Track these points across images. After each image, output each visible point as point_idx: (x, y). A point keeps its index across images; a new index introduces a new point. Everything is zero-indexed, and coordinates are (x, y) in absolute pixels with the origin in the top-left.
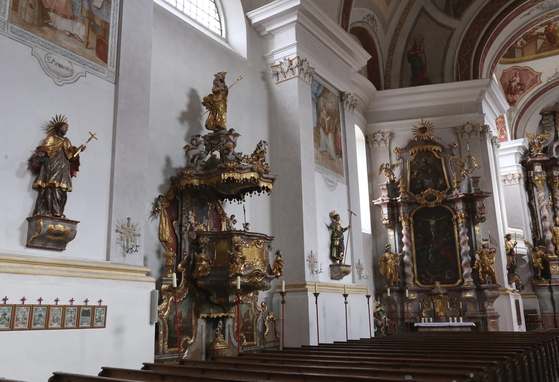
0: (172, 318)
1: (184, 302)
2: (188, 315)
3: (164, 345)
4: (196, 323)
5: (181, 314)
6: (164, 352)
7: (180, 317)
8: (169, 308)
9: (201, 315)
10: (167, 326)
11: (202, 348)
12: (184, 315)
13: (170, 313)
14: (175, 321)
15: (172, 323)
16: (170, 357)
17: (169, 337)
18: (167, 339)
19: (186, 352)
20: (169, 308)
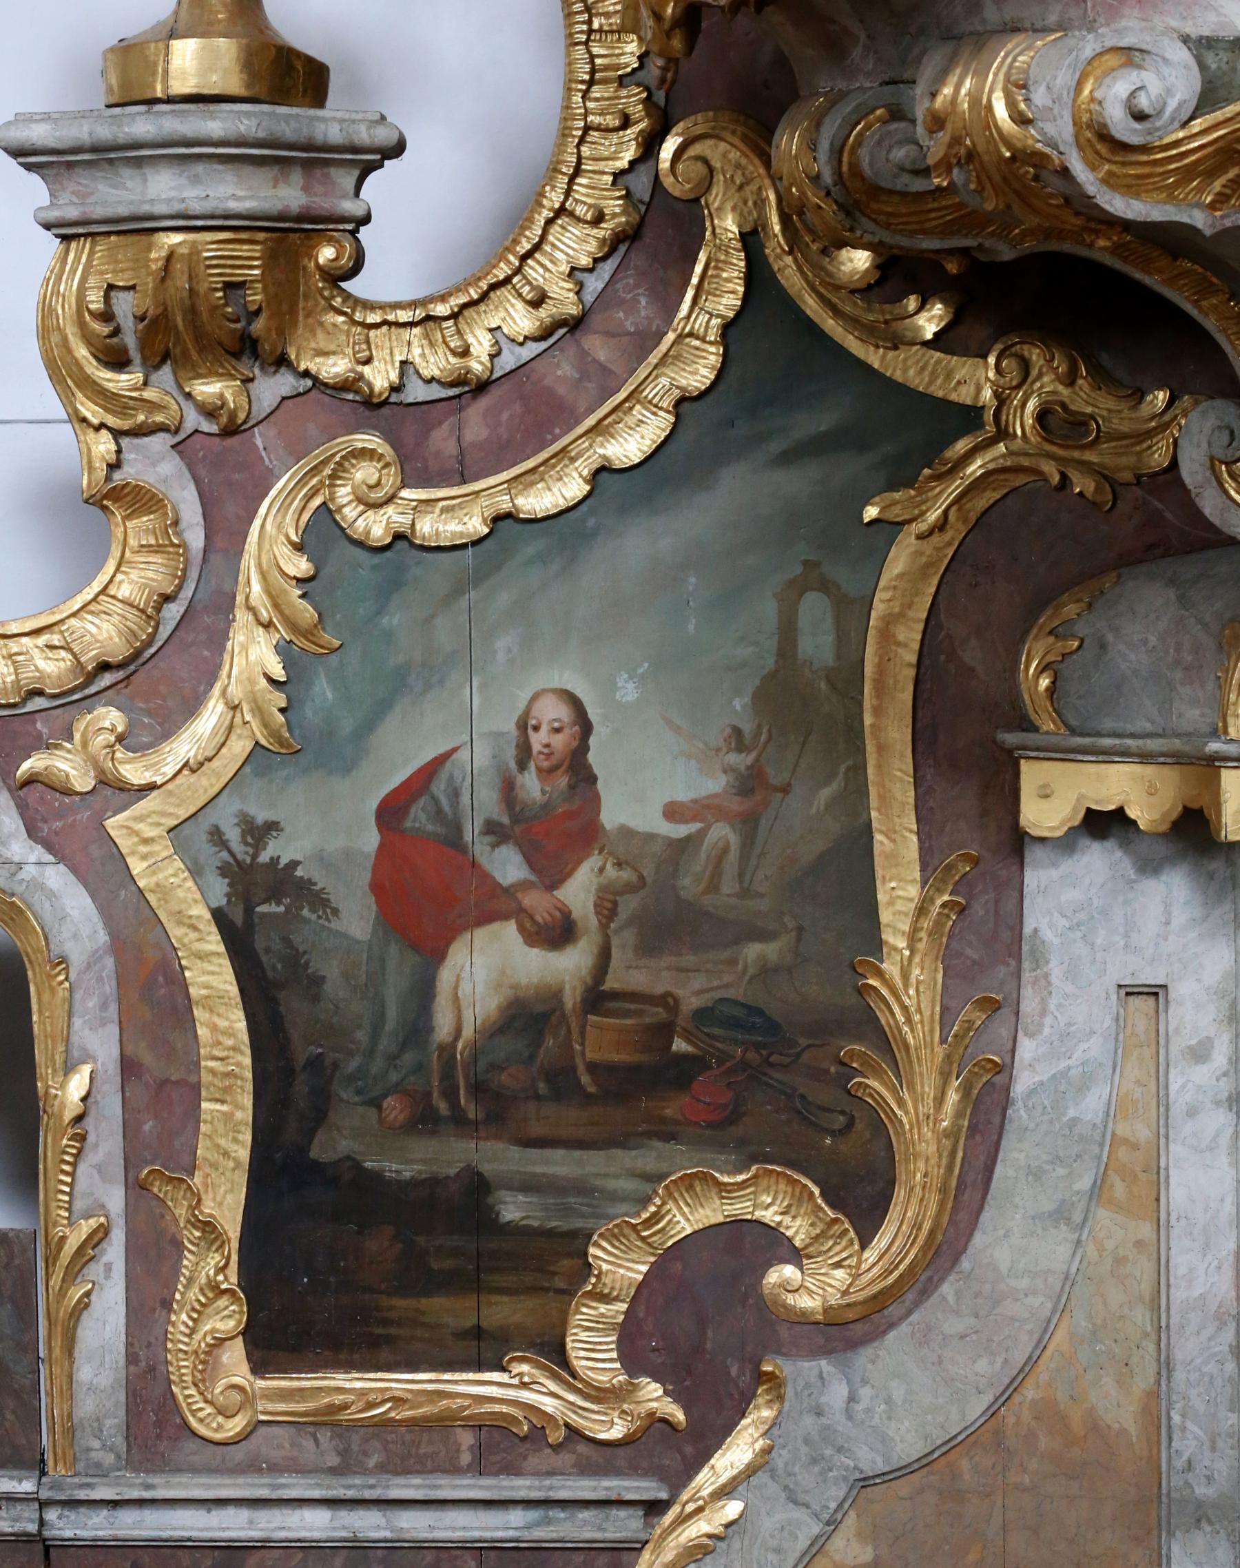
0: (328, 832)
1: (642, 544)
2: (750, 783)
3: (149, 1305)
4: (986, 949)
5: (578, 770)
6: (154, 1425)
7: (560, 823)
8: (253, 654)
9: (1051, 797)
10: (212, 976)
11: (1154, 1413)
12: (652, 782)
13: (293, 746)
14: (426, 888)
15: (356, 918)
16: (314, 1524)
17: (278, 1170)
18: (225, 1200)
19: (735, 1455)
20: (253, 654)
